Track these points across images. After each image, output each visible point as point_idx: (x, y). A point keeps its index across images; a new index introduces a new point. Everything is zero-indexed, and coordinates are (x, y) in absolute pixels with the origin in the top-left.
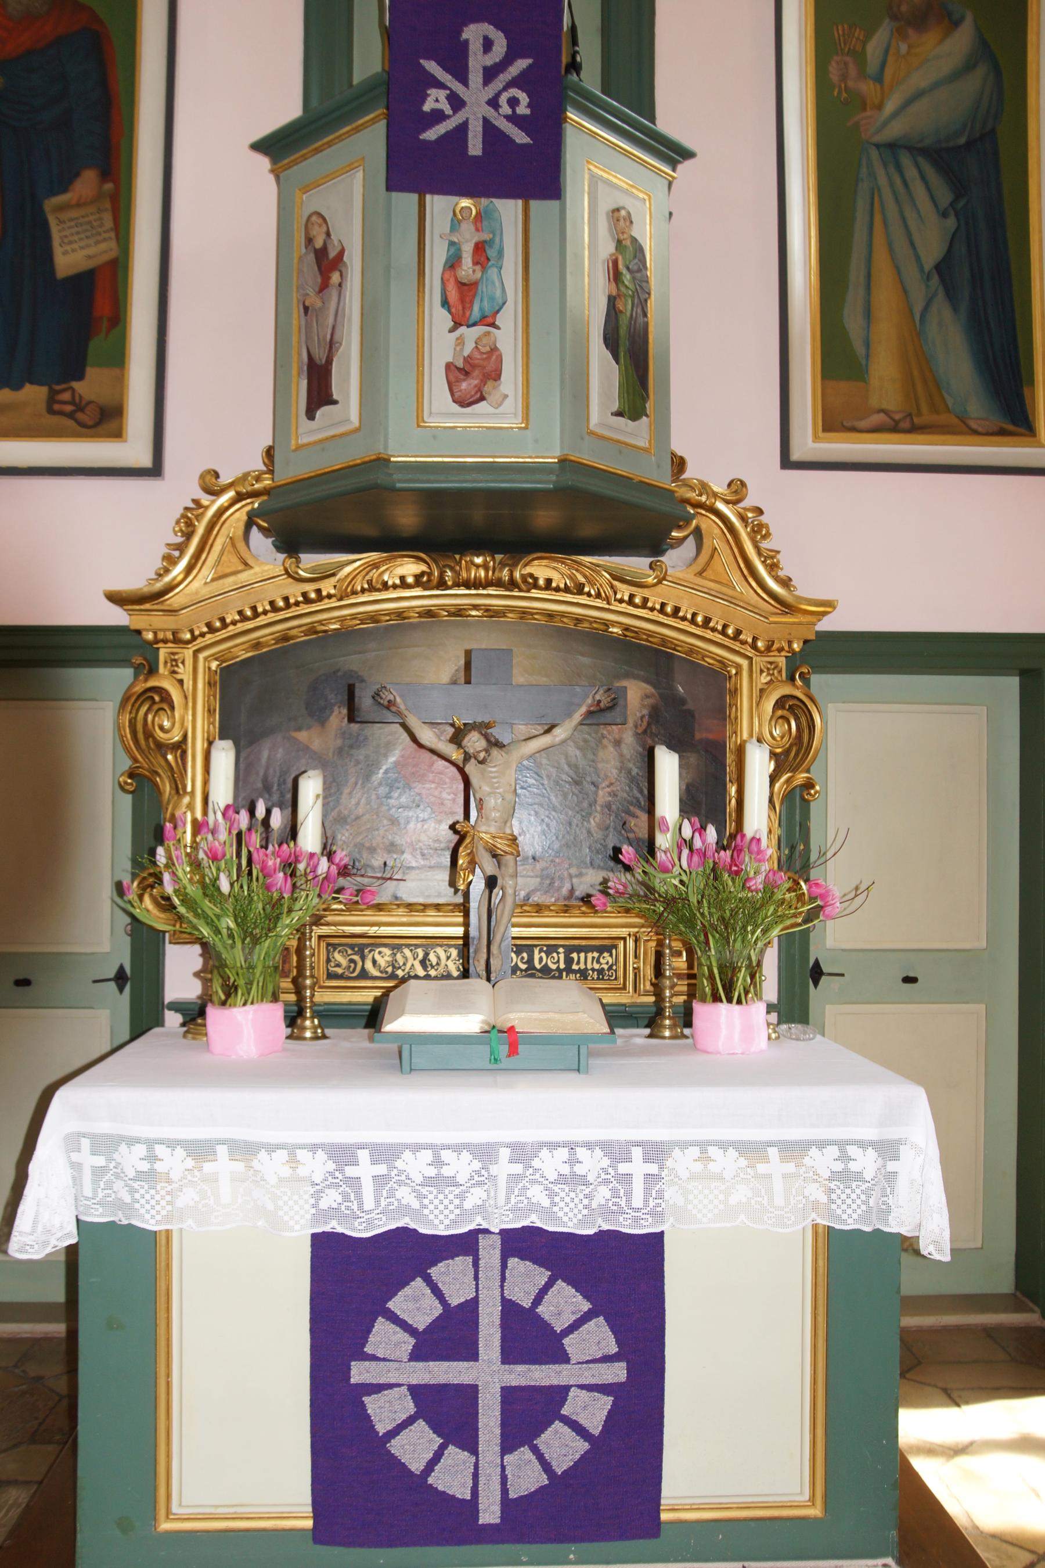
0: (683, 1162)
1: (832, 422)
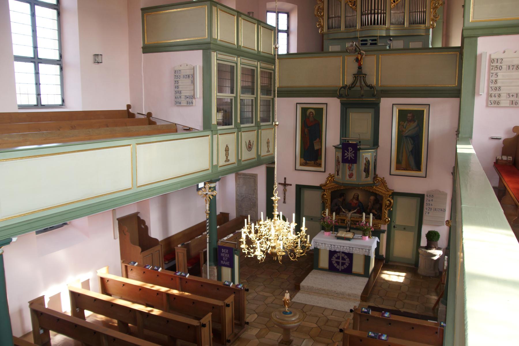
0: (354, 249)
1: (397, 168)
